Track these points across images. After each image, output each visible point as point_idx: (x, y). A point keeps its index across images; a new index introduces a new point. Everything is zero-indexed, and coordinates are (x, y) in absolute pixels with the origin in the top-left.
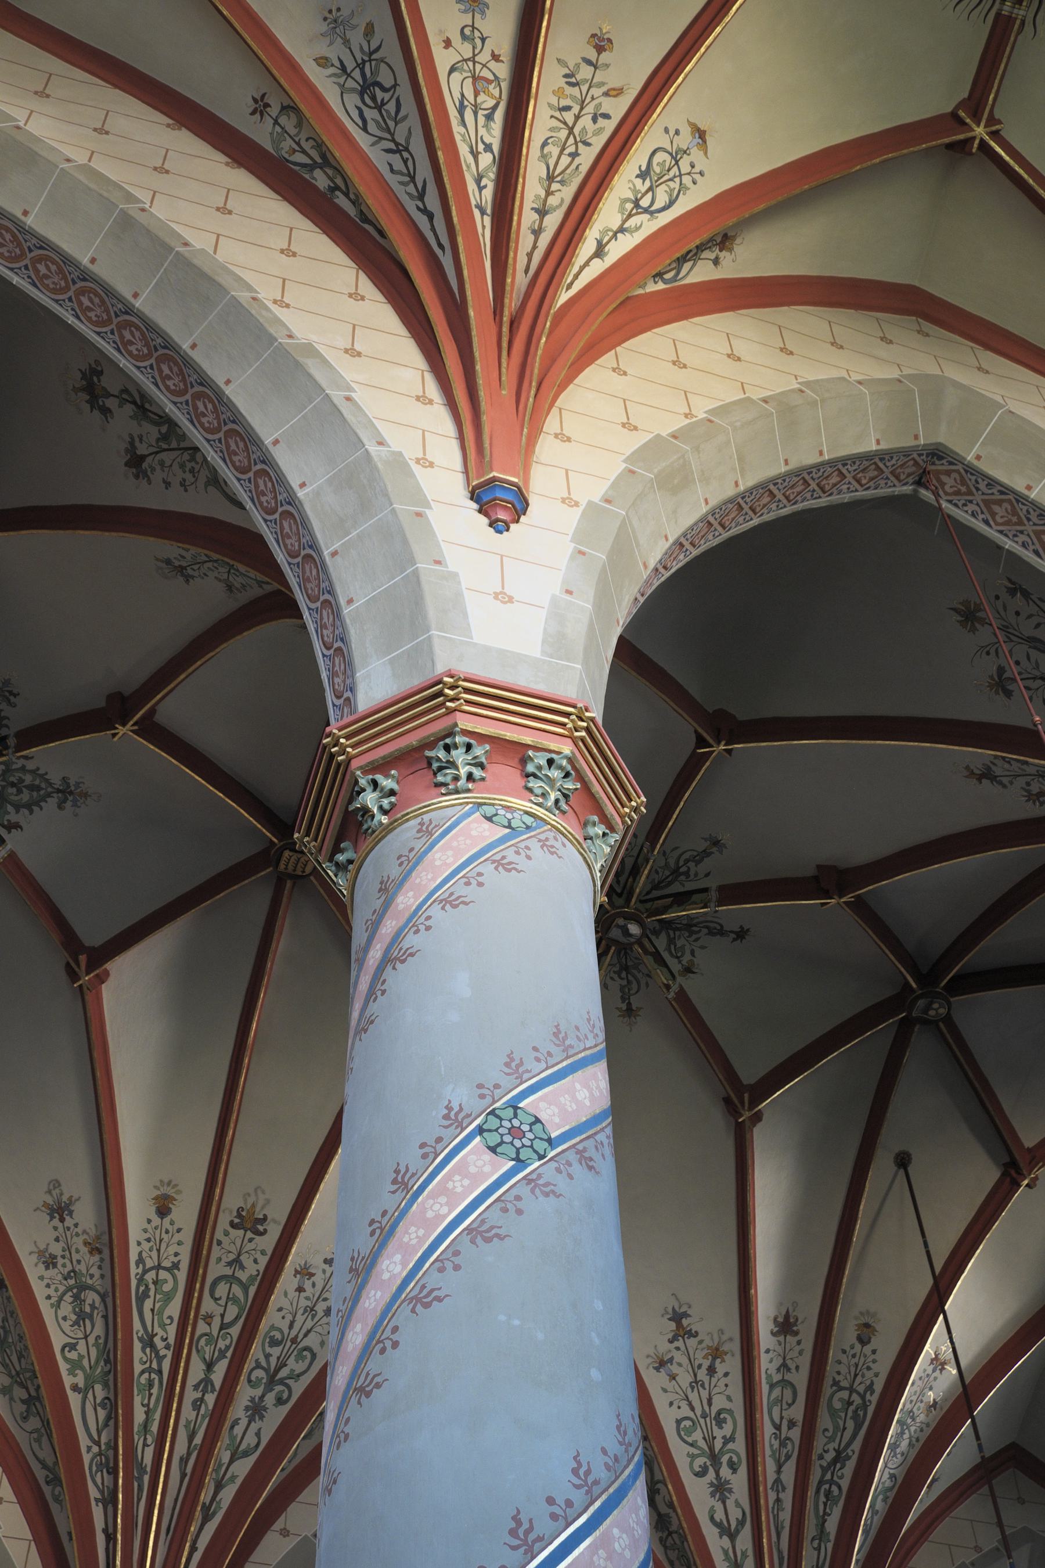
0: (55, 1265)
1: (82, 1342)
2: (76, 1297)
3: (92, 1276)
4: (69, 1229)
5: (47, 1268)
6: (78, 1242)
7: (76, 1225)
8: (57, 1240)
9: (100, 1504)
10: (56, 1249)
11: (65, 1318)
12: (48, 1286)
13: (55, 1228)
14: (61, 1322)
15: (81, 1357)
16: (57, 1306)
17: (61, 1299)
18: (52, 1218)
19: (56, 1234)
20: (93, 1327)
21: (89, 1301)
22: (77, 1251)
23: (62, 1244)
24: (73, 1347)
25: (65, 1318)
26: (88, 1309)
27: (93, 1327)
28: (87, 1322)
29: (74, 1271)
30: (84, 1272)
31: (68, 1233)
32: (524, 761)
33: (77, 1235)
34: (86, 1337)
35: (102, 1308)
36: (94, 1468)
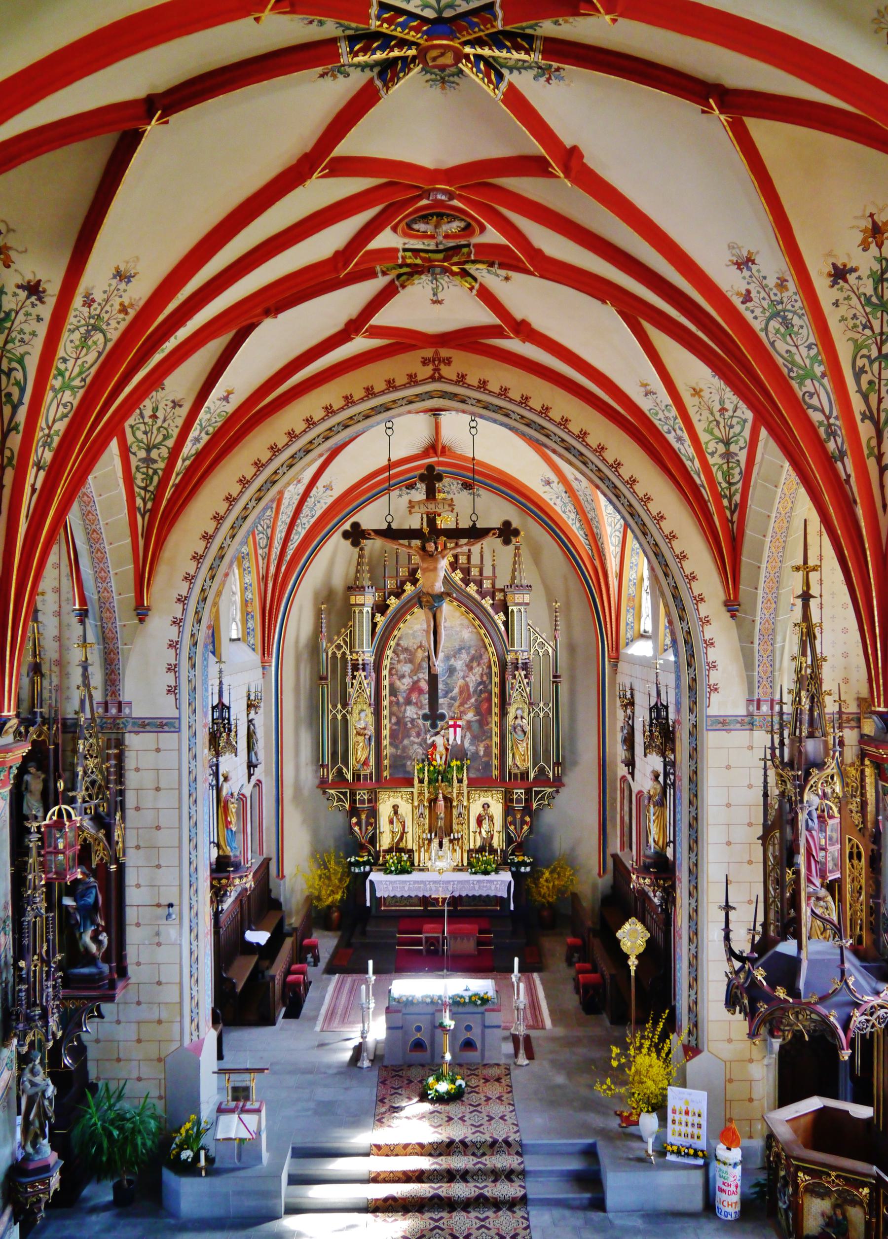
0: (90, 306)
1: (73, 361)
2: (88, 331)
3: (108, 324)
4: (118, 290)
5: (84, 306)
6: (116, 302)
7: (125, 291)
8: (105, 292)
9: (35, 468)
10: (98, 296)
11: (72, 341)
12: (75, 317)
13: (110, 285)
14: (68, 342)
15: (66, 369)
16: (72, 331)
17: (78, 328)
18: (114, 277)
19: (107, 288)
20: (86, 355)
21: (95, 338)
22: (112, 306)
23: (105, 296)
24: (65, 361)
25: (72, 341)
26: (90, 343)
27: (86, 355)
28: (85, 350)
29: (99, 316)
30: (105, 320)
31: (115, 292)
33: (121, 297)
34: (77, 359)
35: (101, 346)
36: (40, 444)
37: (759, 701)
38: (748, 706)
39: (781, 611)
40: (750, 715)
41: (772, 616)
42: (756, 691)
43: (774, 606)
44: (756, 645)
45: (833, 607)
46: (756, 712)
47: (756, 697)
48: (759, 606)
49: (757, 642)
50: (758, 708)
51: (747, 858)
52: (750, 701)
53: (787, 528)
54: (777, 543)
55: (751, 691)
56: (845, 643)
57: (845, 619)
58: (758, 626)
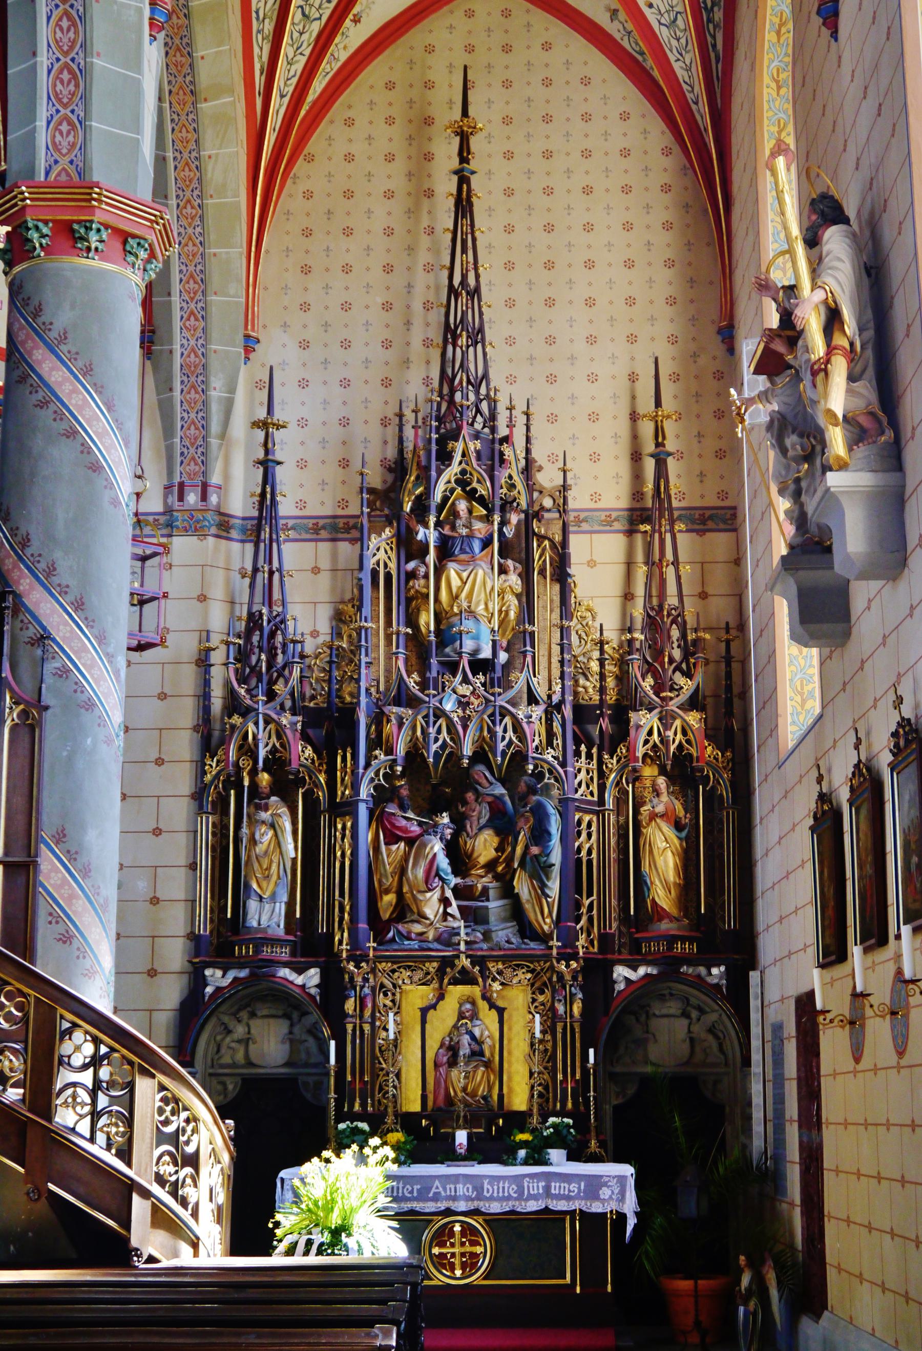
32: (125, 242)
37: (182, 485)
38: (166, 497)
39: (215, 334)
40: (168, 511)
41: (201, 341)
42: (178, 469)
43: (202, 324)
44: (177, 394)
45: (326, 345)
46: (176, 505)
47: (177, 480)
48: (177, 324)
49: (177, 387)
50: (181, 498)
51: (154, 755)
52: (168, 488)
53: (200, 180)
54: (189, 210)
55: (170, 472)
56: (345, 403)
57: (345, 364)
58: (177, 361)
